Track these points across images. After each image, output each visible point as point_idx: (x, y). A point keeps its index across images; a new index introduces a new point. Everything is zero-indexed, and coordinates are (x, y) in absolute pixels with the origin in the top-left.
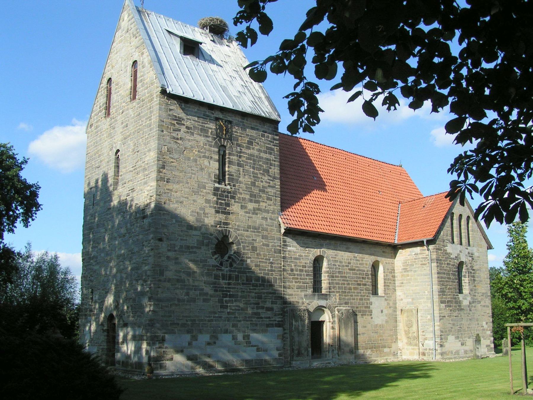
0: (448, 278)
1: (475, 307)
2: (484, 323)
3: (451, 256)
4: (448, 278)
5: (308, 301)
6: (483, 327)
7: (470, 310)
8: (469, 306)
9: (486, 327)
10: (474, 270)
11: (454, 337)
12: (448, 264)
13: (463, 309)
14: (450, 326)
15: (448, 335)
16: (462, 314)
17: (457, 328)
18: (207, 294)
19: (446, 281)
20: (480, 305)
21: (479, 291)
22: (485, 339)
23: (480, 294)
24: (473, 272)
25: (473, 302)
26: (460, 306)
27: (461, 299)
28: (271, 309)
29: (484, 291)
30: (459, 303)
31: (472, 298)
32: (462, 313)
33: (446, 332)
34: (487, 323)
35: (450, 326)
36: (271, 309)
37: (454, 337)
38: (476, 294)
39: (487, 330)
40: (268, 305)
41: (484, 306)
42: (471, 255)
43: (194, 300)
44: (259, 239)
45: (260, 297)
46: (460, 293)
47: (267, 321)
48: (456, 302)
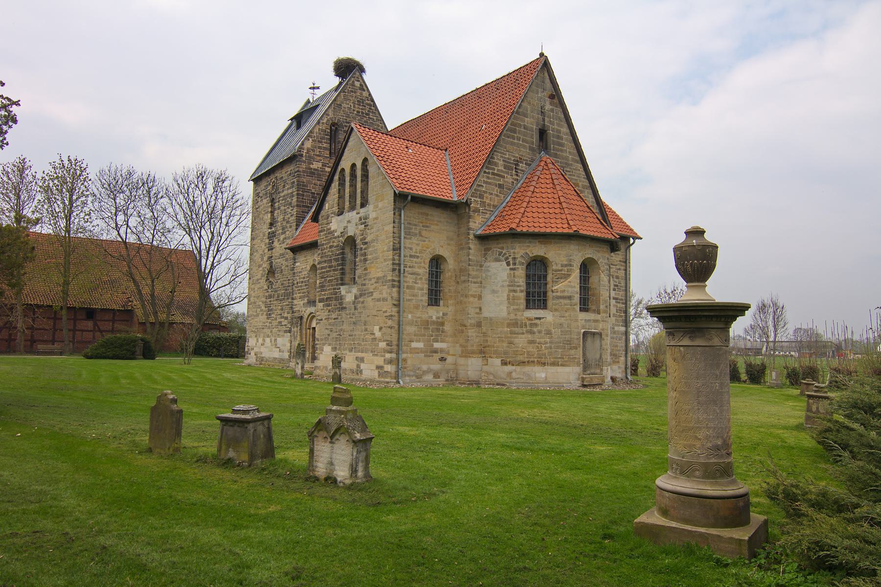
0: (330, 267)
1: (363, 302)
2: (377, 328)
3: (336, 234)
4: (330, 267)
5: (304, 309)
6: (374, 334)
7: (355, 309)
8: (354, 303)
9: (378, 334)
10: (366, 243)
11: (330, 347)
12: (331, 247)
13: (345, 308)
14: (327, 332)
15: (324, 344)
16: (344, 315)
17: (334, 335)
18: (262, 310)
19: (327, 272)
20: (370, 299)
21: (371, 276)
22: (376, 355)
23: (373, 281)
24: (364, 247)
25: (361, 295)
26: (341, 304)
27: (343, 293)
28: (286, 318)
29: (380, 274)
30: (340, 299)
31: (359, 290)
32: (343, 313)
33: (322, 340)
34: (381, 329)
35: (327, 332)
36: (286, 318)
37: (330, 347)
38: (367, 282)
39: (380, 340)
40: (286, 315)
41: (379, 300)
42: (364, 221)
43: (258, 315)
44: (284, 262)
45: (282, 309)
46: (342, 284)
47: (284, 328)
48: (336, 299)
